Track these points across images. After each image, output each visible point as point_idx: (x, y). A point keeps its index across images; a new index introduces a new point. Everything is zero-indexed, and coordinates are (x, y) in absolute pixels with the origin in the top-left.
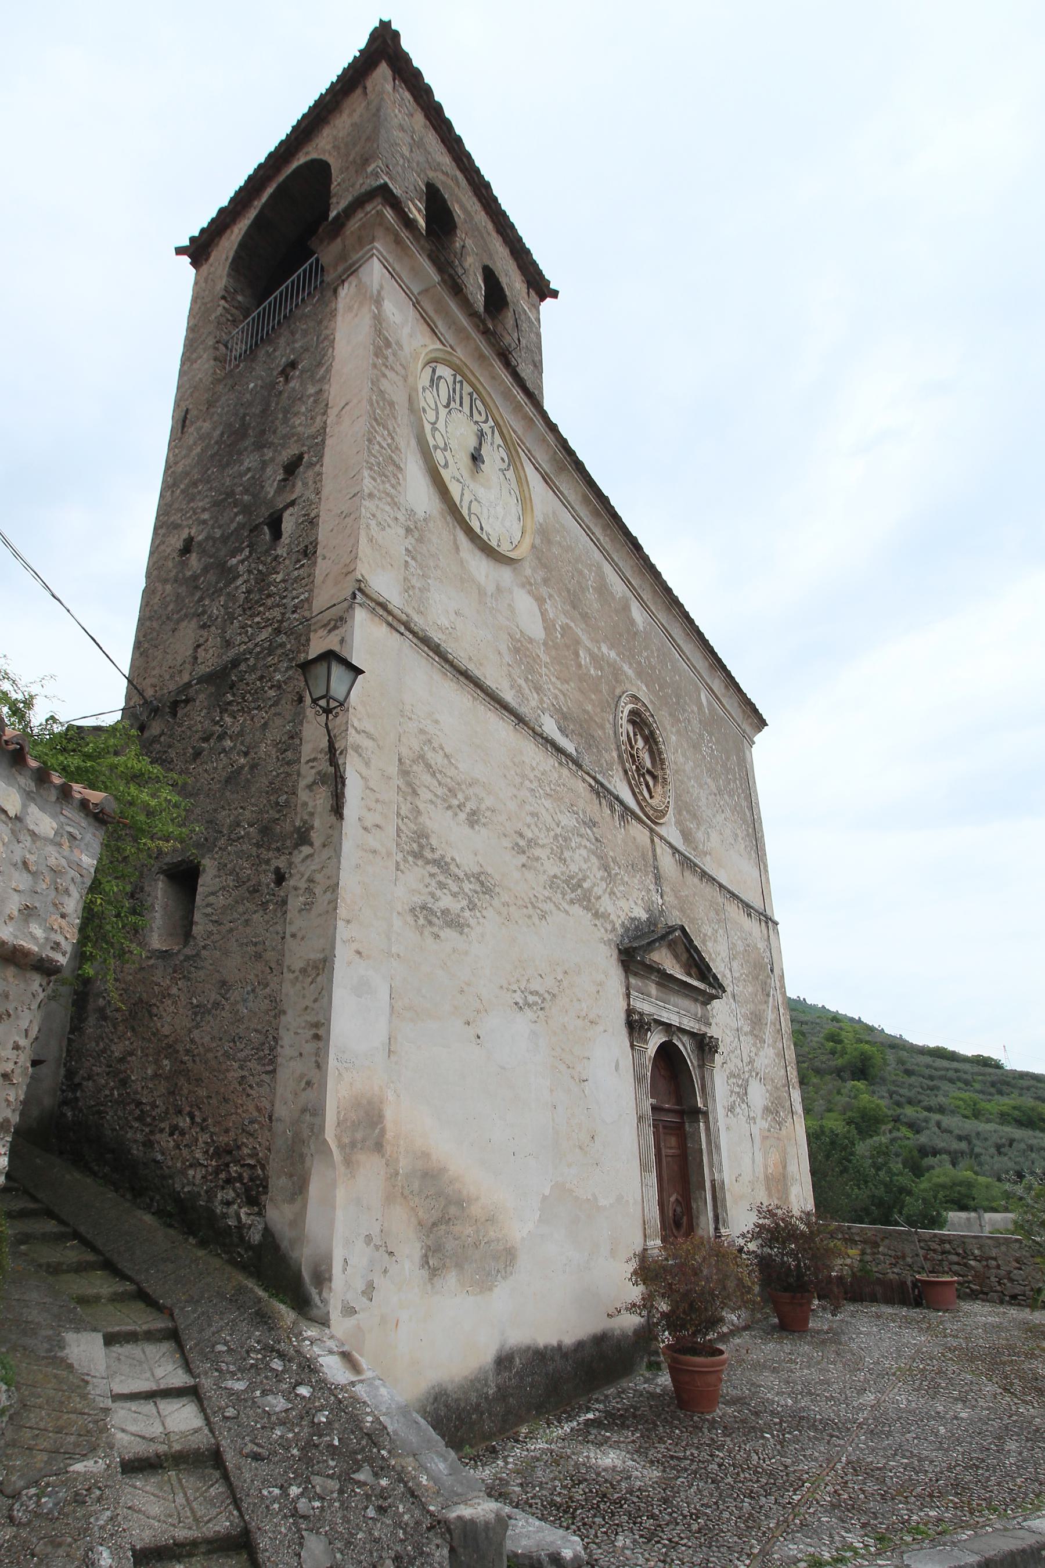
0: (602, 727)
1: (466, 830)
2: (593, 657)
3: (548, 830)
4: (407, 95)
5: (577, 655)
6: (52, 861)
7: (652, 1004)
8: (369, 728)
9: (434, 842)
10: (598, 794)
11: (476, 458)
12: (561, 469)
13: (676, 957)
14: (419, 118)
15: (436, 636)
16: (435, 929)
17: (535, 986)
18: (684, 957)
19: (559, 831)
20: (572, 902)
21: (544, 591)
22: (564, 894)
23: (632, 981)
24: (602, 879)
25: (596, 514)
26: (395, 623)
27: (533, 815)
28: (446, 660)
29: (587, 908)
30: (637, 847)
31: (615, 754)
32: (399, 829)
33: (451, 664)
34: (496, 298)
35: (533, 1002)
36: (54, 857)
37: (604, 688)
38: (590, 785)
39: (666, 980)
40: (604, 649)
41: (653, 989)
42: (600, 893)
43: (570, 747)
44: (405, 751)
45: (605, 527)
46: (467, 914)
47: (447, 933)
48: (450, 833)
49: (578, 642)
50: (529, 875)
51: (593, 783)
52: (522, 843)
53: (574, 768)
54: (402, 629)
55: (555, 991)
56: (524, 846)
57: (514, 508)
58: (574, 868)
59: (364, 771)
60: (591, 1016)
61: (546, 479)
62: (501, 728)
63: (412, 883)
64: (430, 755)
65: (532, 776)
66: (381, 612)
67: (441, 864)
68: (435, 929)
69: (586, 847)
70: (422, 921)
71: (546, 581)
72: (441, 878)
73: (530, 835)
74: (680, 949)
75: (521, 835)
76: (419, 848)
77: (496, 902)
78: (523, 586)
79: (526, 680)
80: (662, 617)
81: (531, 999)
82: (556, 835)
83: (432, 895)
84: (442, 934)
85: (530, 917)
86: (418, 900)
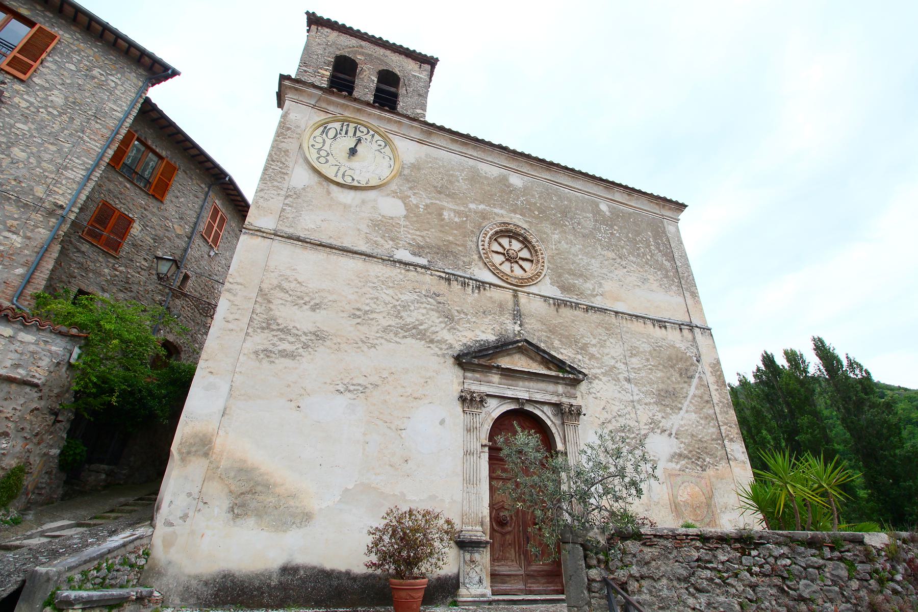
0: (464, 246)
1: (310, 313)
2: (458, 213)
3: (386, 304)
4: (329, 30)
5: (441, 215)
6: (31, 350)
7: (493, 385)
8: (239, 280)
9: (280, 321)
10: (449, 280)
11: (353, 152)
12: (430, 134)
13: (531, 358)
14: (335, 34)
15: (302, 235)
16: (272, 359)
17: (361, 381)
18: (539, 358)
19: (397, 303)
20: (405, 337)
21: (410, 193)
22: (396, 334)
23: (469, 375)
24: (441, 322)
25: (466, 144)
26: (268, 236)
27: (372, 299)
29: (420, 339)
30: (494, 302)
31: (476, 257)
32: (251, 320)
33: (310, 243)
34: (388, 79)
35: (352, 388)
36: (32, 348)
37: (469, 226)
40: (472, 206)
41: (496, 378)
42: (437, 329)
43: (423, 261)
44: (264, 286)
45: (475, 148)
46: (301, 350)
47: (287, 362)
48: (287, 314)
49: (442, 208)
50: (363, 328)
51: (443, 275)
52: (358, 313)
53: (423, 270)
54: (273, 237)
55: (380, 383)
56: (360, 315)
57: (386, 162)
58: (409, 320)
59: (232, 298)
60: (416, 395)
61: (420, 142)
62: (356, 264)
63: (261, 340)
64: (285, 285)
65: (376, 281)
66: (258, 233)
67: (286, 331)
68: (272, 359)
70: (262, 356)
71: (410, 188)
72: (283, 336)
73: (367, 308)
74: (533, 355)
75: (359, 310)
76: (268, 325)
77: (328, 343)
78: (388, 195)
79: (383, 237)
81: (352, 388)
82: (395, 306)
83: (274, 345)
84: (277, 361)
85: (359, 348)
86: (261, 347)
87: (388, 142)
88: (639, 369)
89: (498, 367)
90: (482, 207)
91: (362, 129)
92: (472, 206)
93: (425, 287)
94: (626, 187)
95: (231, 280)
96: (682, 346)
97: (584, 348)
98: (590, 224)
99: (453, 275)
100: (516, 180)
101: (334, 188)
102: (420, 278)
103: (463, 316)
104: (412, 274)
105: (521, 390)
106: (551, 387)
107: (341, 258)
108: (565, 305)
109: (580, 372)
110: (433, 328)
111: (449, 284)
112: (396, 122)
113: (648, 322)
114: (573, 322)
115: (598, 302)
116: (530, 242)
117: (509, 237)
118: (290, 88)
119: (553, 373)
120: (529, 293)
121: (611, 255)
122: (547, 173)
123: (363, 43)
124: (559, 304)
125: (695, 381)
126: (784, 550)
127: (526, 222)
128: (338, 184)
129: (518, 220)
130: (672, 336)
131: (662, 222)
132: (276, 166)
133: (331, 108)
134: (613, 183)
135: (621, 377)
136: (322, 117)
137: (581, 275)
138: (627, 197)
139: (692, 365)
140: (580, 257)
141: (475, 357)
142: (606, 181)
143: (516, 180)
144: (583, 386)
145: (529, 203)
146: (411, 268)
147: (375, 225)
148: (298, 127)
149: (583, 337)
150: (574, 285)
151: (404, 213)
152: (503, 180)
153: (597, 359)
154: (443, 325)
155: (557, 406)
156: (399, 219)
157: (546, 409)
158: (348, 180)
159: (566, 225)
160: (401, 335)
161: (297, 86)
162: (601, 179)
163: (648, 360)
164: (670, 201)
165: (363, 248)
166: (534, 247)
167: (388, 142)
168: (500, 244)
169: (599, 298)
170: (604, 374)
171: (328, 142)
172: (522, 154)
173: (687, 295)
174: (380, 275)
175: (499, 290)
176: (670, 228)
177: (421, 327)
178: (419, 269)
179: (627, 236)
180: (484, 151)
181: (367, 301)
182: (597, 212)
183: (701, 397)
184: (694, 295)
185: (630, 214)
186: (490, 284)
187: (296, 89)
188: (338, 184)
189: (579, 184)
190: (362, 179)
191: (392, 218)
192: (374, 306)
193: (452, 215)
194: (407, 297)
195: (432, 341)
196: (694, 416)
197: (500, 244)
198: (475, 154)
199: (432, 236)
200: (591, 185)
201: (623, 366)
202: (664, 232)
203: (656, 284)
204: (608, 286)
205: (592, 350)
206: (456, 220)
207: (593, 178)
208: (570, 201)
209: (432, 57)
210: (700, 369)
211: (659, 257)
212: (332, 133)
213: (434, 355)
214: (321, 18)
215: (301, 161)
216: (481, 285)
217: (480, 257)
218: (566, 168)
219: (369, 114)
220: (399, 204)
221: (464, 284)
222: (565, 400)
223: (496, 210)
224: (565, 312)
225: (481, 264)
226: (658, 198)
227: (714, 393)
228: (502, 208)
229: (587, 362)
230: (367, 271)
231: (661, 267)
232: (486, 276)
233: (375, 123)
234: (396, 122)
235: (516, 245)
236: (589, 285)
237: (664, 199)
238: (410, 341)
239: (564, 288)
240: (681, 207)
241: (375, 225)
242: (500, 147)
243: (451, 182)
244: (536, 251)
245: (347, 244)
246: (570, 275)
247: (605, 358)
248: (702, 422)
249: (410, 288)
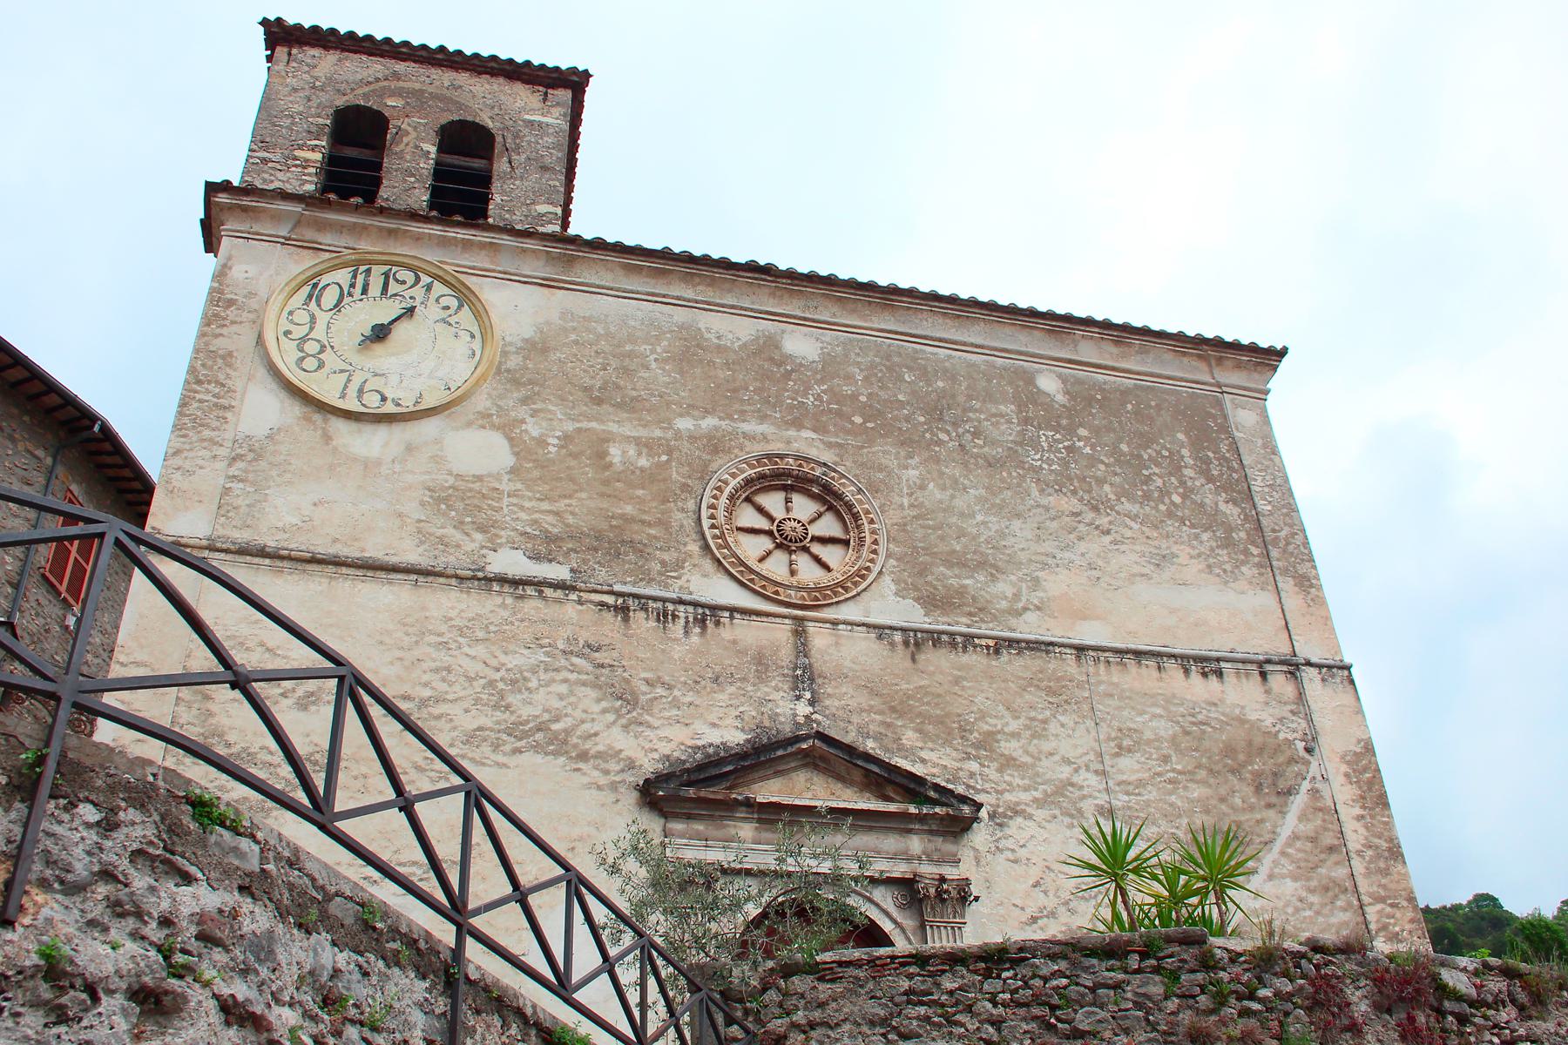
0: (663, 523)
3: (470, 679)
4: (316, 52)
5: (602, 455)
9: (231, 738)
10: (623, 611)
11: (380, 333)
12: (570, 261)
13: (839, 778)
14: (332, 58)
15: (271, 543)
18: (857, 775)
19: (498, 676)
21: (523, 412)
22: (496, 747)
23: (678, 826)
24: (604, 711)
28: (275, 556)
29: (555, 754)
30: (742, 653)
31: (694, 547)
37: (676, 475)
38: (602, 604)
39: (769, 814)
40: (684, 424)
41: (746, 830)
42: (597, 728)
43: (560, 572)
45: (687, 278)
49: (606, 439)
51: (610, 600)
53: (559, 593)
57: (462, 346)
58: (526, 712)
65: (444, 628)
69: (566, 681)
71: (525, 401)
73: (427, 693)
78: (469, 424)
79: (459, 525)
80: (887, 321)
82: (492, 683)
87: (465, 296)
88: (1141, 783)
89: (749, 804)
90: (709, 422)
91: (404, 274)
92: (684, 424)
93: (566, 632)
94: (1106, 325)
95: (122, 658)
96: (1267, 718)
97: (987, 743)
98: (1007, 432)
99: (635, 596)
100: (801, 345)
101: (339, 426)
102: (551, 611)
103: (660, 691)
104: (532, 606)
105: (815, 856)
106: (891, 842)
107: (360, 586)
108: (937, 643)
109: (964, 799)
110: (585, 727)
111: (626, 619)
112: (483, 246)
113: (1170, 665)
114: (957, 681)
115: (1029, 627)
116: (839, 496)
117: (785, 488)
118: (231, 207)
119: (892, 807)
120: (835, 623)
121: (1068, 503)
122: (887, 315)
123: (401, 67)
124: (916, 641)
125: (1299, 802)
126: (1062, 965)
127: (830, 445)
128: (348, 415)
129: (807, 445)
130: (1242, 696)
131: (1219, 404)
132: (205, 394)
133: (327, 239)
134: (1068, 318)
135: (1088, 806)
136: (306, 262)
137: (982, 564)
138: (1114, 350)
139: (1292, 760)
140: (979, 518)
141: (690, 784)
142: (1050, 316)
143: (801, 345)
144: (980, 836)
145: (837, 397)
146: (530, 591)
147: (439, 500)
148: (251, 295)
149: (983, 716)
150: (961, 592)
151: (509, 460)
152: (767, 349)
153: (1021, 767)
154: (611, 717)
155: (907, 886)
156: (498, 477)
157: (879, 894)
158: (372, 401)
159: (940, 443)
160: (508, 748)
161: (246, 201)
162: (1032, 313)
163: (1165, 759)
164: (1235, 346)
165: (412, 554)
166: (849, 506)
167: (465, 296)
168: (761, 510)
169: (1031, 617)
170: (1040, 803)
171: (323, 318)
172: (812, 279)
173: (1286, 584)
174: (453, 614)
175: (756, 624)
176: (1242, 417)
177: (555, 727)
178: (548, 592)
179: (1115, 451)
180: (712, 282)
181: (425, 678)
182: (1029, 397)
183: (1313, 840)
184: (1307, 583)
185: (1125, 393)
186: (733, 610)
187: (245, 209)
188: (348, 415)
189: (974, 333)
190: (404, 396)
191: (479, 478)
192: (443, 687)
193: (632, 452)
194: (519, 659)
195: (583, 756)
196: (1289, 887)
197: (761, 510)
198: (689, 293)
199: (582, 509)
200: (1008, 330)
201: (1093, 780)
202: (1225, 428)
203: (1197, 566)
204: (1056, 584)
205: (1009, 747)
206: (643, 462)
207: (1012, 311)
208: (953, 378)
209: (574, 71)
210: (1314, 769)
211: (1207, 495)
212: (330, 297)
213: (589, 786)
214: (299, 27)
215: (261, 372)
216: (708, 614)
217: (706, 547)
218: (934, 297)
219: (418, 238)
220: (498, 441)
221: (664, 617)
222: (927, 869)
223: (746, 427)
224: (938, 660)
225: (708, 565)
226: (1200, 342)
227: (1350, 826)
228: (763, 418)
229: (994, 775)
230: (424, 608)
231: (1212, 521)
232: (725, 592)
233: (432, 256)
234: (483, 246)
235: (804, 508)
236: (1004, 587)
237: (1218, 343)
238: (529, 758)
239: (931, 602)
240: (1270, 357)
241: (439, 500)
242: (752, 267)
243: (627, 372)
244: (856, 517)
245: (374, 550)
246: (949, 564)
247: (1045, 762)
249: (528, 637)
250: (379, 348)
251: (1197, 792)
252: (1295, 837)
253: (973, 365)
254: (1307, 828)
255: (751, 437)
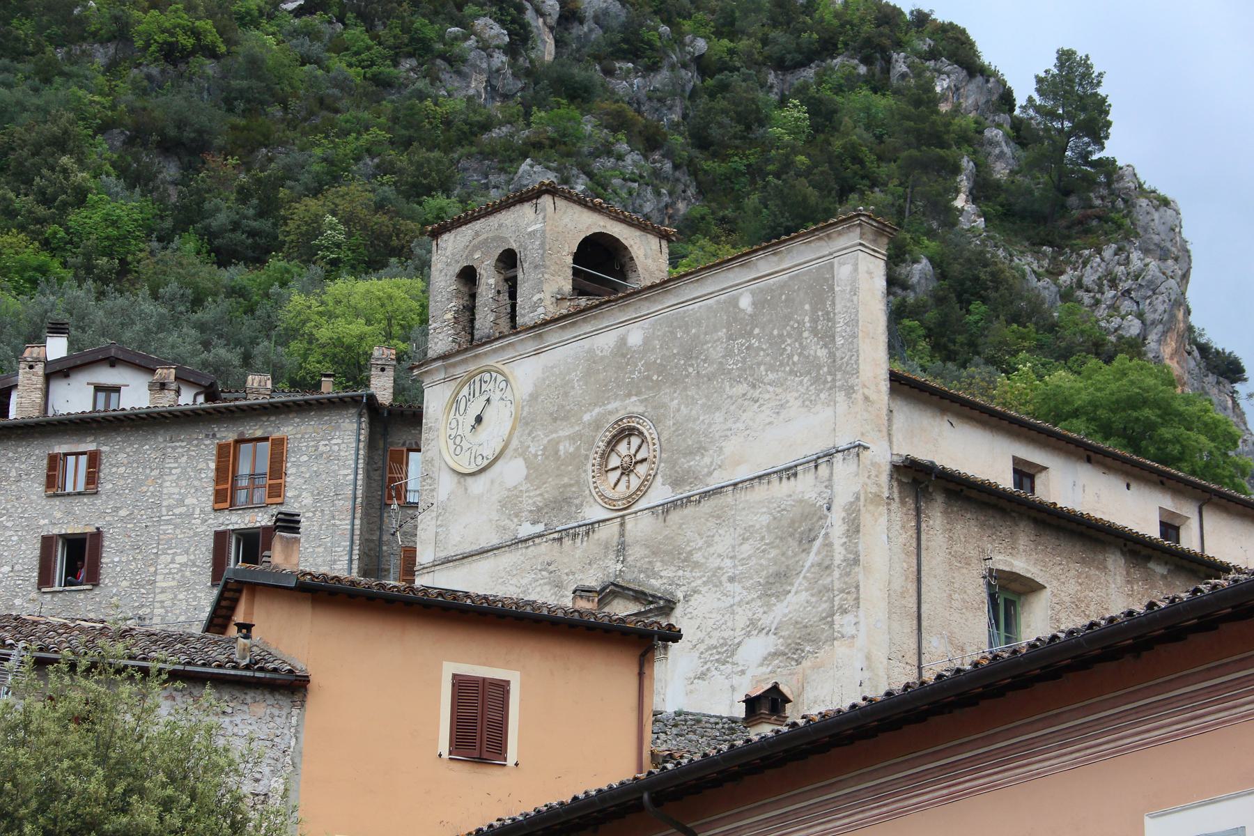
108: (675, 506)
138: (775, 259)
149: (689, 541)
163: (763, 538)
178: (537, 541)
191: (515, 487)
223: (610, 407)
224: (675, 516)
229: (688, 574)
245: (484, 544)
247: (711, 560)
248: (813, 599)
250: (480, 428)
251: (773, 553)
252: (812, 566)
253: (709, 308)
254: (818, 559)
255: (610, 413)
